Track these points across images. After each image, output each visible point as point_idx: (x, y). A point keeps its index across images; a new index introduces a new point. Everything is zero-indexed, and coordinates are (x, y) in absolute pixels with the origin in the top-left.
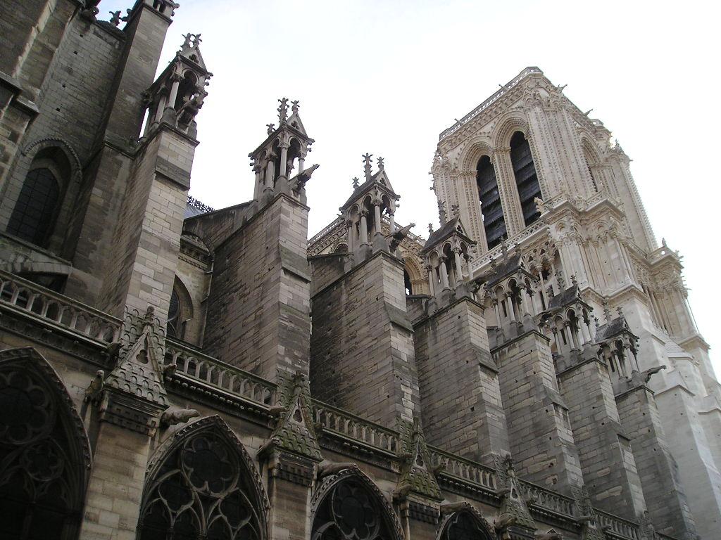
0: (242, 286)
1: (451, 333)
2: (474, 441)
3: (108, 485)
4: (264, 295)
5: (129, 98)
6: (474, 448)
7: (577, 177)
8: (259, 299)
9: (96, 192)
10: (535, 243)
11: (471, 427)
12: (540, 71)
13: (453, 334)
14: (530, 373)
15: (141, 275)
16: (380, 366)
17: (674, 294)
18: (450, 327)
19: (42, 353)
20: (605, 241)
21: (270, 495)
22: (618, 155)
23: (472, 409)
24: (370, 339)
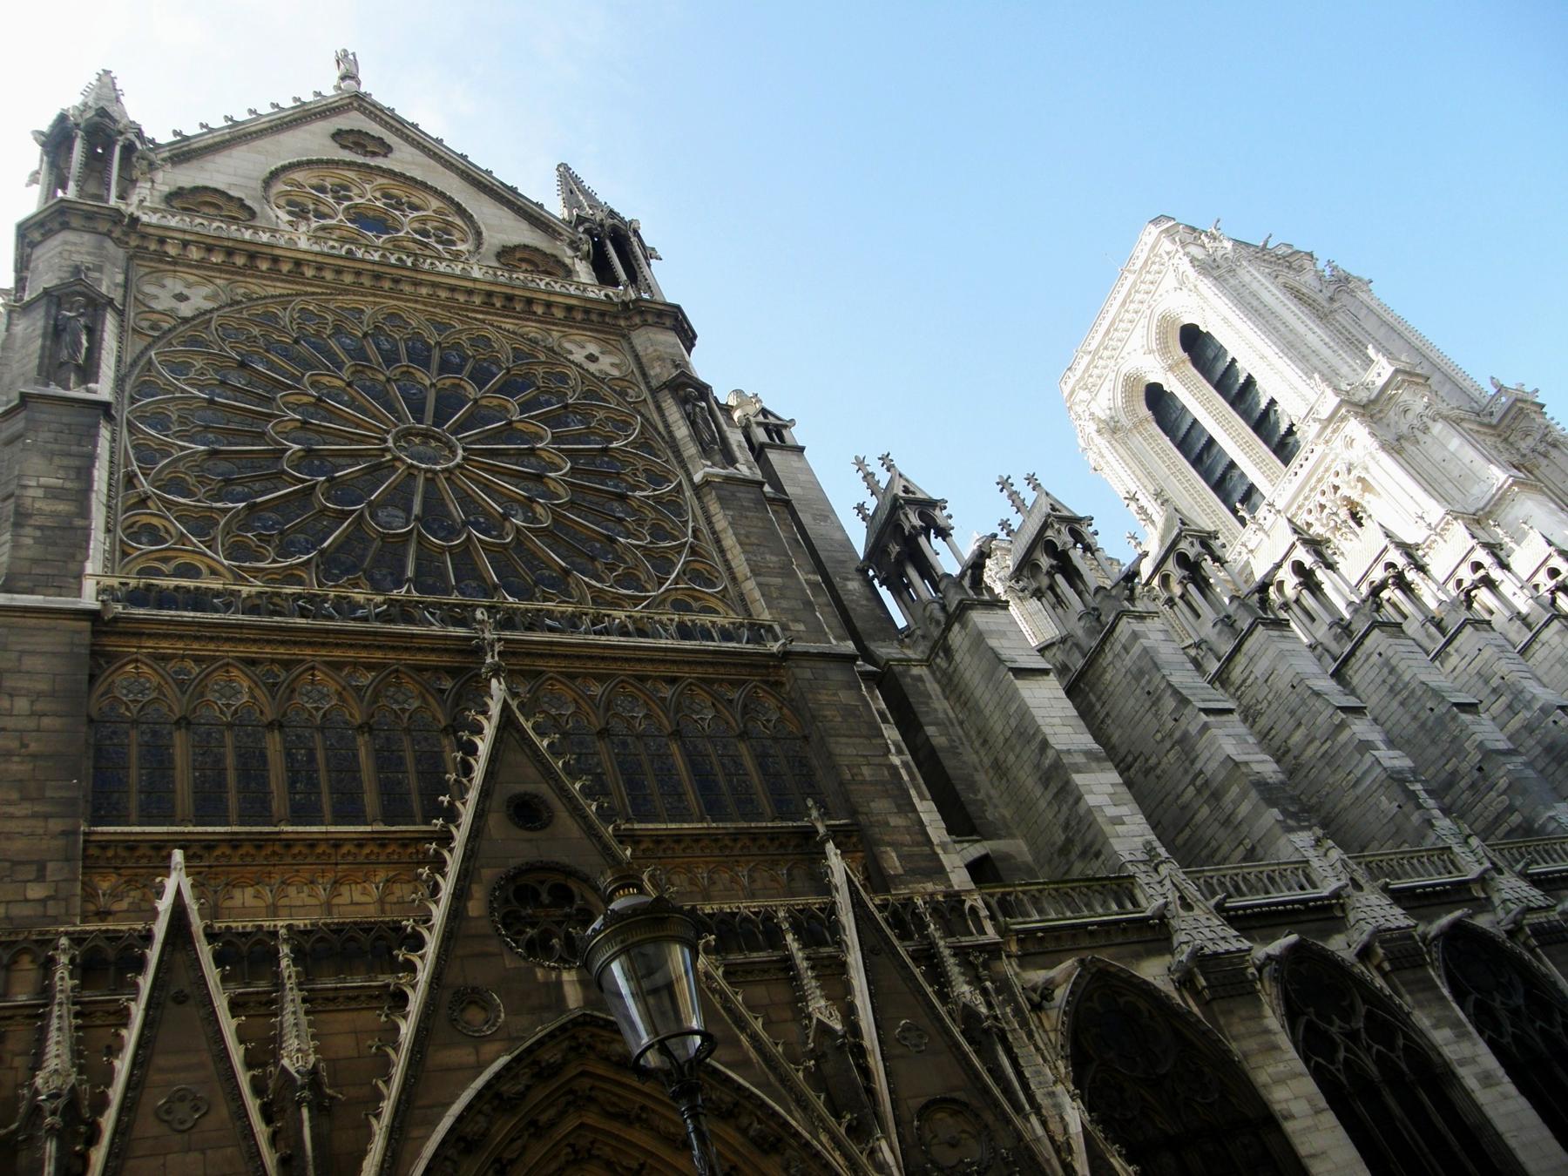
0: (1135, 760)
1: (1379, 680)
2: (1511, 809)
3: (1270, 1070)
4: (1192, 756)
6: (1516, 819)
7: (1327, 353)
8: (1187, 763)
9: (931, 730)
10: (1319, 480)
11: (1493, 793)
12: (1170, 219)
13: (1384, 681)
14: (1495, 682)
16: (1358, 773)
17: (1554, 453)
18: (1372, 675)
19: (1104, 956)
20: (1426, 430)
21: (1401, 997)
22: (1343, 283)
23: (1480, 769)
24: (1317, 743)
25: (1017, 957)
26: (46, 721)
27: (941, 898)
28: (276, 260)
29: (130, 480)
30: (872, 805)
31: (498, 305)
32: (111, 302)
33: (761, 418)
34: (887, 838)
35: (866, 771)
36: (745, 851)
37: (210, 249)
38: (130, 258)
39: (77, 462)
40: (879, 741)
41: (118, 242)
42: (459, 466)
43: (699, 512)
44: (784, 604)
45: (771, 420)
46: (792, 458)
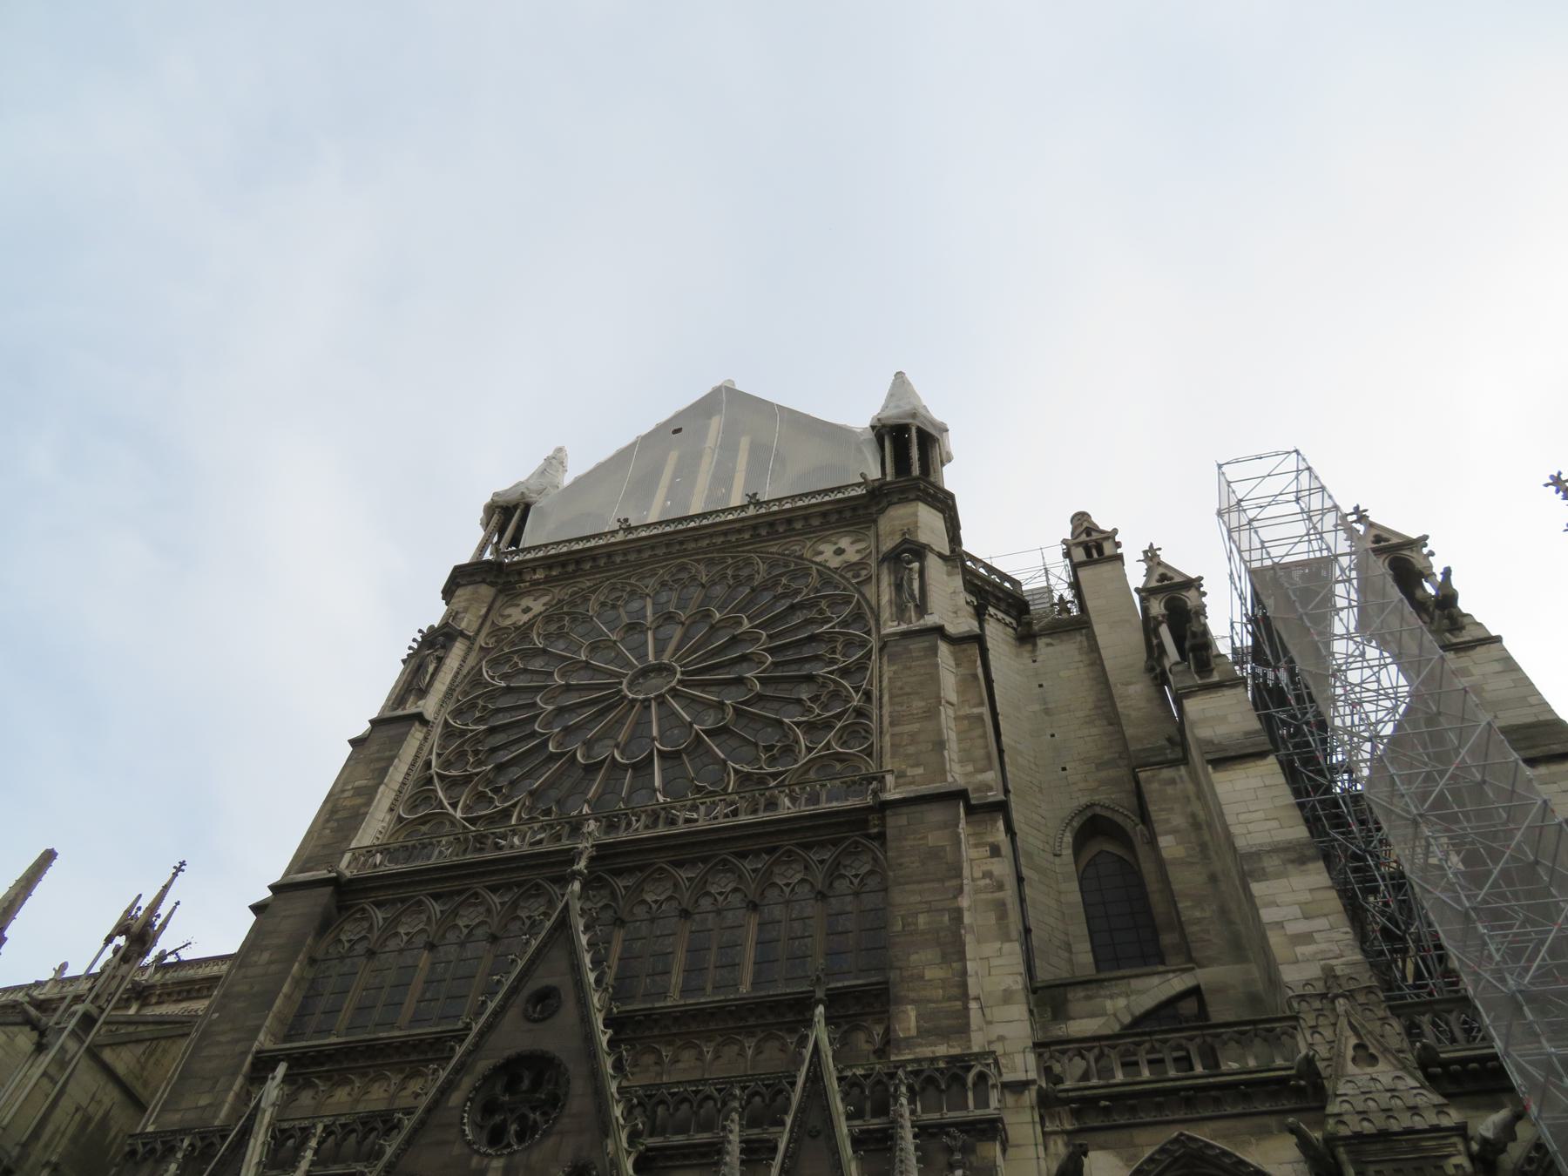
5: (1132, 689)
15: (1280, 925)
25: (1068, 1133)
26: (273, 968)
27: (942, 1065)
28: (594, 559)
29: (428, 764)
30: (914, 957)
31: (764, 532)
32: (462, 634)
33: (1084, 537)
34: (912, 995)
35: (922, 920)
36: (761, 1021)
37: (550, 567)
38: (500, 592)
39: (383, 764)
40: (954, 882)
41: (492, 584)
42: (673, 689)
43: (876, 672)
44: (911, 750)
45: (1095, 536)
46: (1105, 570)
